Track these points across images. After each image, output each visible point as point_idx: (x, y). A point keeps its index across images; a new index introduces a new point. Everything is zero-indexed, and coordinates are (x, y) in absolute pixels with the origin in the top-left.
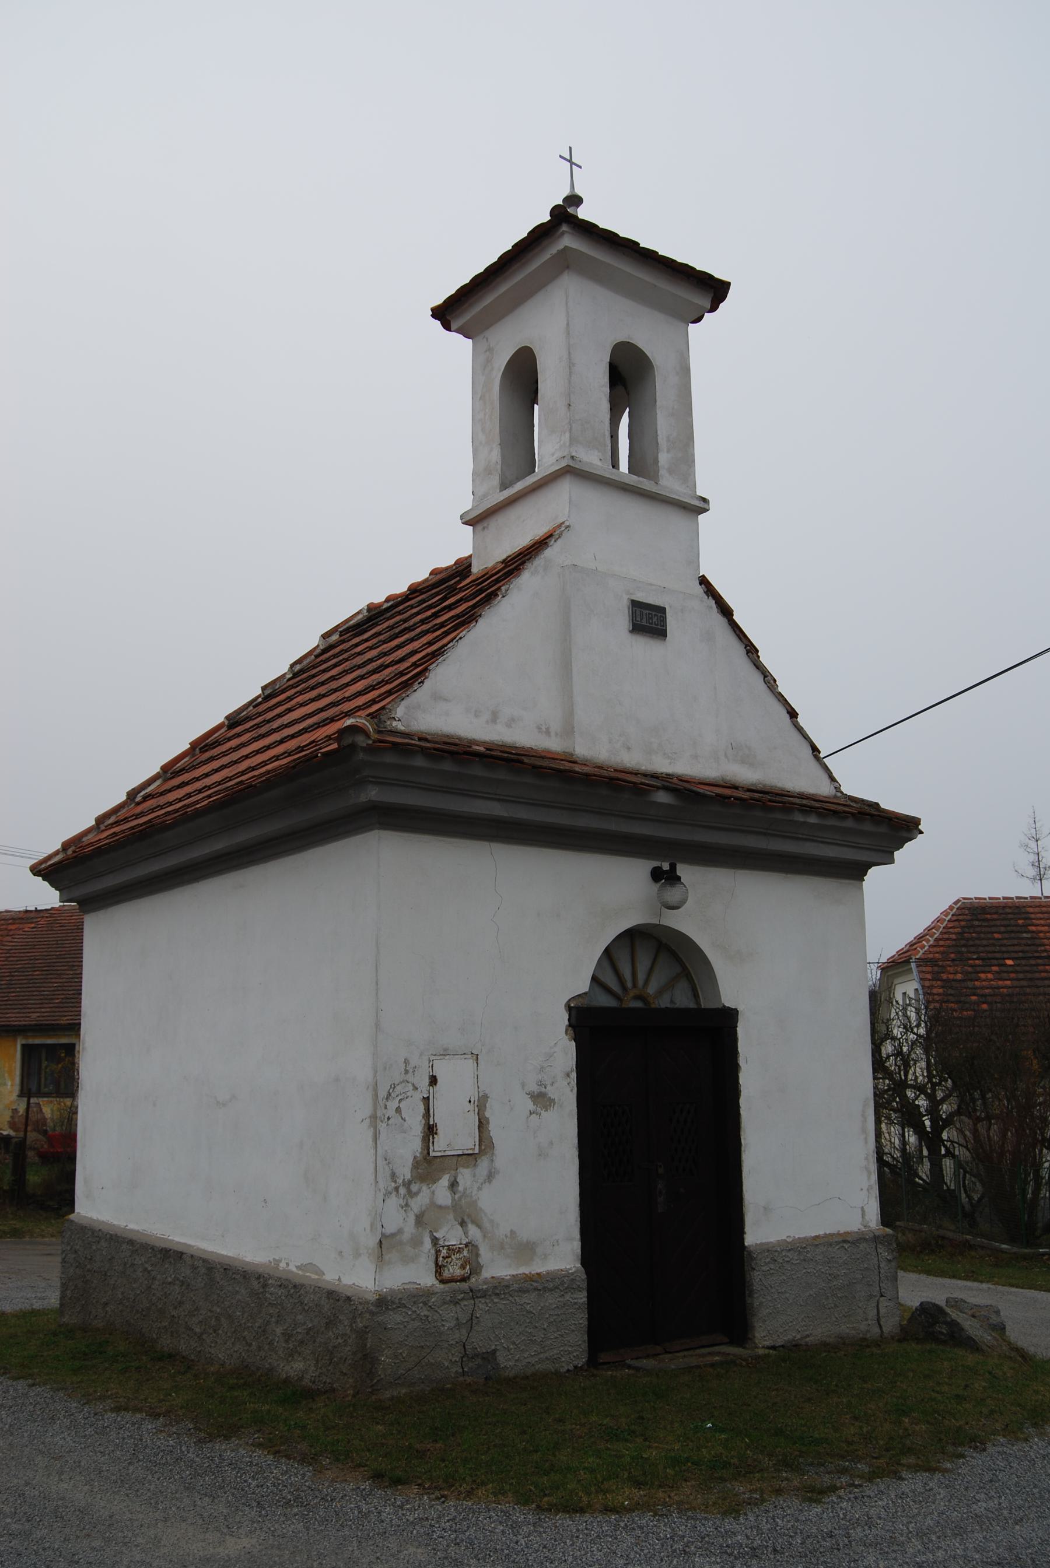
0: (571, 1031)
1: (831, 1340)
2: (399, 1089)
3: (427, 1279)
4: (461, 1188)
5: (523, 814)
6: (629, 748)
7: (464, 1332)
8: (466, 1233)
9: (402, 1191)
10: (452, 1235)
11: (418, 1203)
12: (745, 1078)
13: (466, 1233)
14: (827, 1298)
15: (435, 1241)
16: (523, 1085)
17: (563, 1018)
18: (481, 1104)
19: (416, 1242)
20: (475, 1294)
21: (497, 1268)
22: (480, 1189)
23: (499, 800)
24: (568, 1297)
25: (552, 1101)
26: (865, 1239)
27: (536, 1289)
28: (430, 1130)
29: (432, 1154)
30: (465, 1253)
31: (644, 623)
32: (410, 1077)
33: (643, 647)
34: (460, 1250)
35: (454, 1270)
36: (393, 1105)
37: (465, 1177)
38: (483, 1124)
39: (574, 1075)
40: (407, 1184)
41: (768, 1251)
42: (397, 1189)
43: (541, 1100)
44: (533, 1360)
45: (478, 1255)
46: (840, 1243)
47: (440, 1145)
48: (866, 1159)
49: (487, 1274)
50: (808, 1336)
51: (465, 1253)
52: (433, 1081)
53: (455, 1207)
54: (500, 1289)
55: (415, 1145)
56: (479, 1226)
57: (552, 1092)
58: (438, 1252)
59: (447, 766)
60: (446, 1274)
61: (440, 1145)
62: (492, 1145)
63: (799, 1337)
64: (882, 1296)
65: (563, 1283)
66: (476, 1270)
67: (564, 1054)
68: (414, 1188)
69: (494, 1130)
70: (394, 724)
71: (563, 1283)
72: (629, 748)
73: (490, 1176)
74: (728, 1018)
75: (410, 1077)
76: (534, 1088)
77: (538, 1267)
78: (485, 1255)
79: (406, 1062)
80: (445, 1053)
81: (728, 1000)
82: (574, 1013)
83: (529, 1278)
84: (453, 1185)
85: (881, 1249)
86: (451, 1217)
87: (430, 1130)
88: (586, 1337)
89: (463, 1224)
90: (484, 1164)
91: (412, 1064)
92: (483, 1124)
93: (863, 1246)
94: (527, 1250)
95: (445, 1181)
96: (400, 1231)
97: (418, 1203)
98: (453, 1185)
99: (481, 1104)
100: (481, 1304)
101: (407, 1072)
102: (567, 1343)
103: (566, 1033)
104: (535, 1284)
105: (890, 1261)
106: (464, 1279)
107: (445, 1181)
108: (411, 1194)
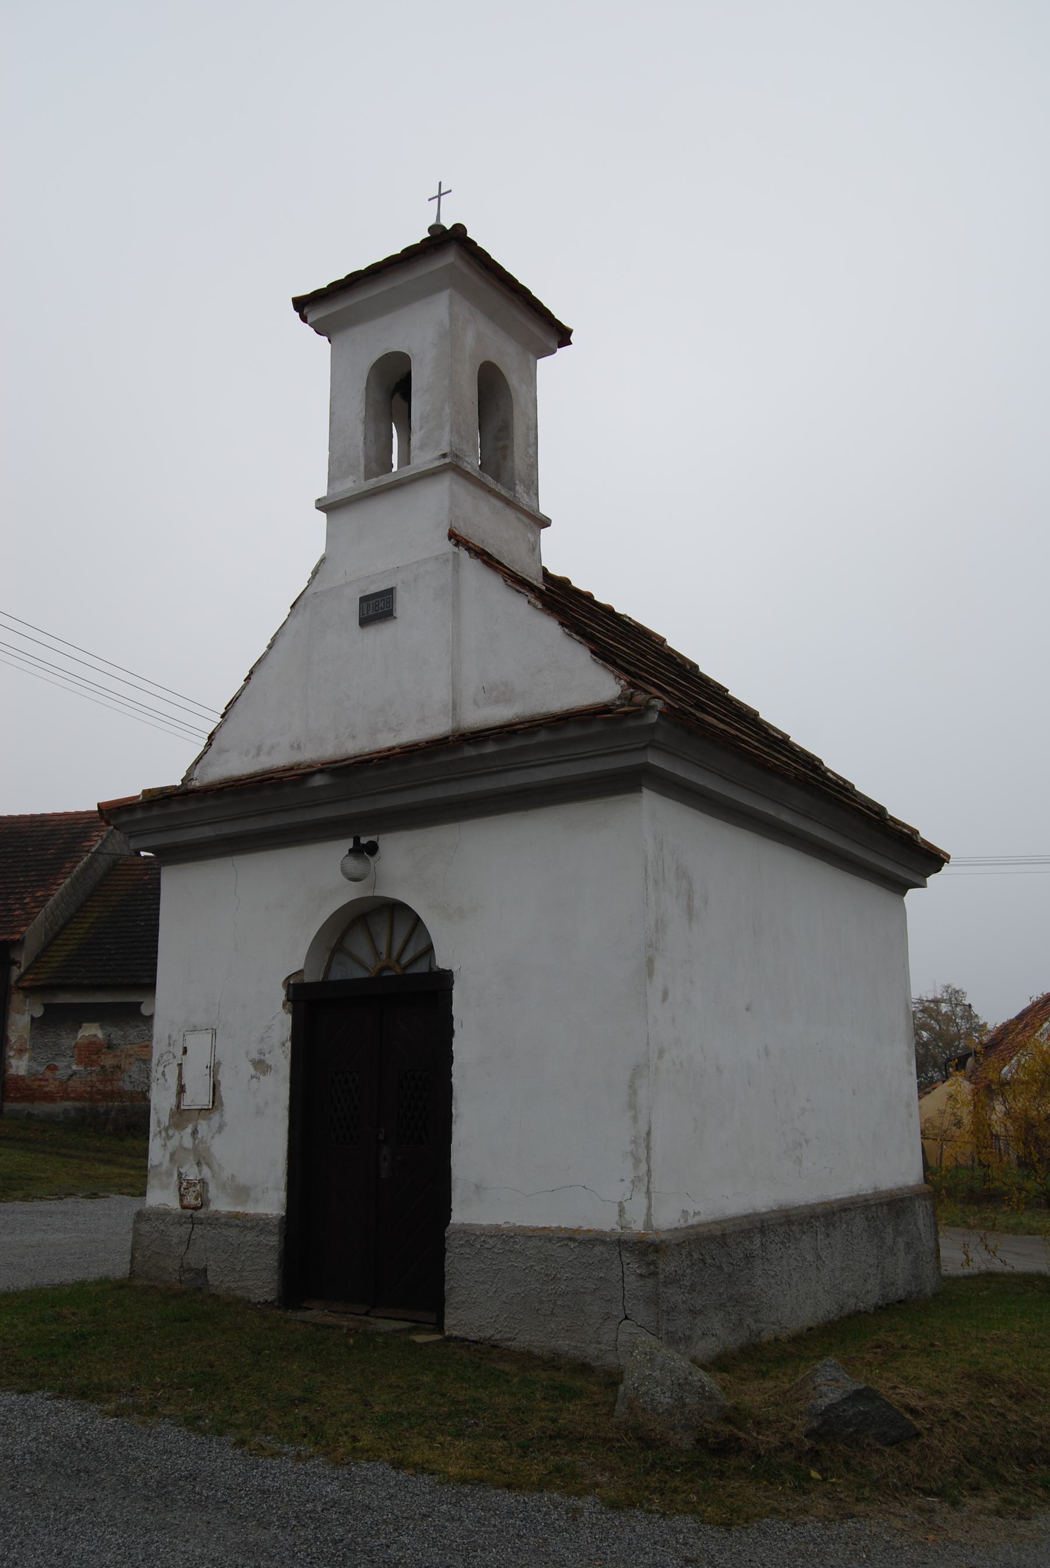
0: (289, 1005)
1: (536, 1351)
2: (165, 1058)
3: (174, 1204)
4: (199, 1136)
5: (226, 829)
6: (354, 737)
7: (184, 1248)
8: (200, 1172)
9: (163, 1134)
10: (192, 1173)
11: (173, 1144)
12: (458, 1045)
13: (200, 1172)
14: (541, 1302)
15: (180, 1174)
16: (247, 1053)
17: (281, 994)
18: (214, 1069)
19: (169, 1174)
20: (193, 1221)
21: (221, 1204)
22: (213, 1137)
23: (208, 824)
24: (261, 1238)
25: (269, 1067)
26: (604, 1242)
27: (237, 1226)
28: (181, 1089)
29: (183, 1107)
30: (198, 1187)
31: (371, 613)
32: (171, 1049)
33: (381, 634)
34: (195, 1185)
35: (190, 1200)
36: (161, 1069)
37: (203, 1126)
38: (215, 1088)
39: (289, 1044)
40: (167, 1129)
41: (465, 1232)
42: (160, 1132)
43: (261, 1066)
44: (233, 1285)
45: (208, 1191)
46: (563, 1239)
47: (187, 1101)
48: (634, 1141)
49: (213, 1207)
50: (509, 1339)
51: (198, 1187)
52: (185, 1051)
53: (195, 1149)
54: (216, 1221)
55: (173, 1100)
56: (210, 1168)
57: (269, 1059)
58: (181, 1183)
59: (155, 812)
60: (185, 1202)
61: (187, 1101)
62: (222, 1104)
63: (498, 1337)
64: (627, 1318)
65: (258, 1225)
66: (205, 1204)
67: (282, 1024)
68: (171, 1132)
69: (224, 1090)
70: (193, 783)
71: (258, 1225)
72: (354, 737)
73: (221, 1128)
74: (443, 981)
75: (171, 1049)
76: (255, 1056)
77: (252, 1209)
78: (213, 1192)
79: (170, 1037)
80: (194, 1030)
81: (442, 961)
82: (291, 990)
83: (237, 1216)
84: (195, 1132)
85: (627, 1257)
86: (191, 1158)
87: (181, 1089)
88: (276, 1277)
89: (199, 1164)
90: (216, 1117)
91: (174, 1038)
92: (215, 1088)
93: (598, 1249)
94: (242, 1192)
95: (189, 1130)
96: (161, 1164)
97: (173, 1144)
98: (195, 1132)
99: (214, 1069)
100: (198, 1229)
101: (170, 1045)
102: (258, 1277)
103: (284, 1005)
104: (237, 1222)
105: (641, 1275)
106: (196, 1208)
107: (189, 1130)
108: (169, 1137)
